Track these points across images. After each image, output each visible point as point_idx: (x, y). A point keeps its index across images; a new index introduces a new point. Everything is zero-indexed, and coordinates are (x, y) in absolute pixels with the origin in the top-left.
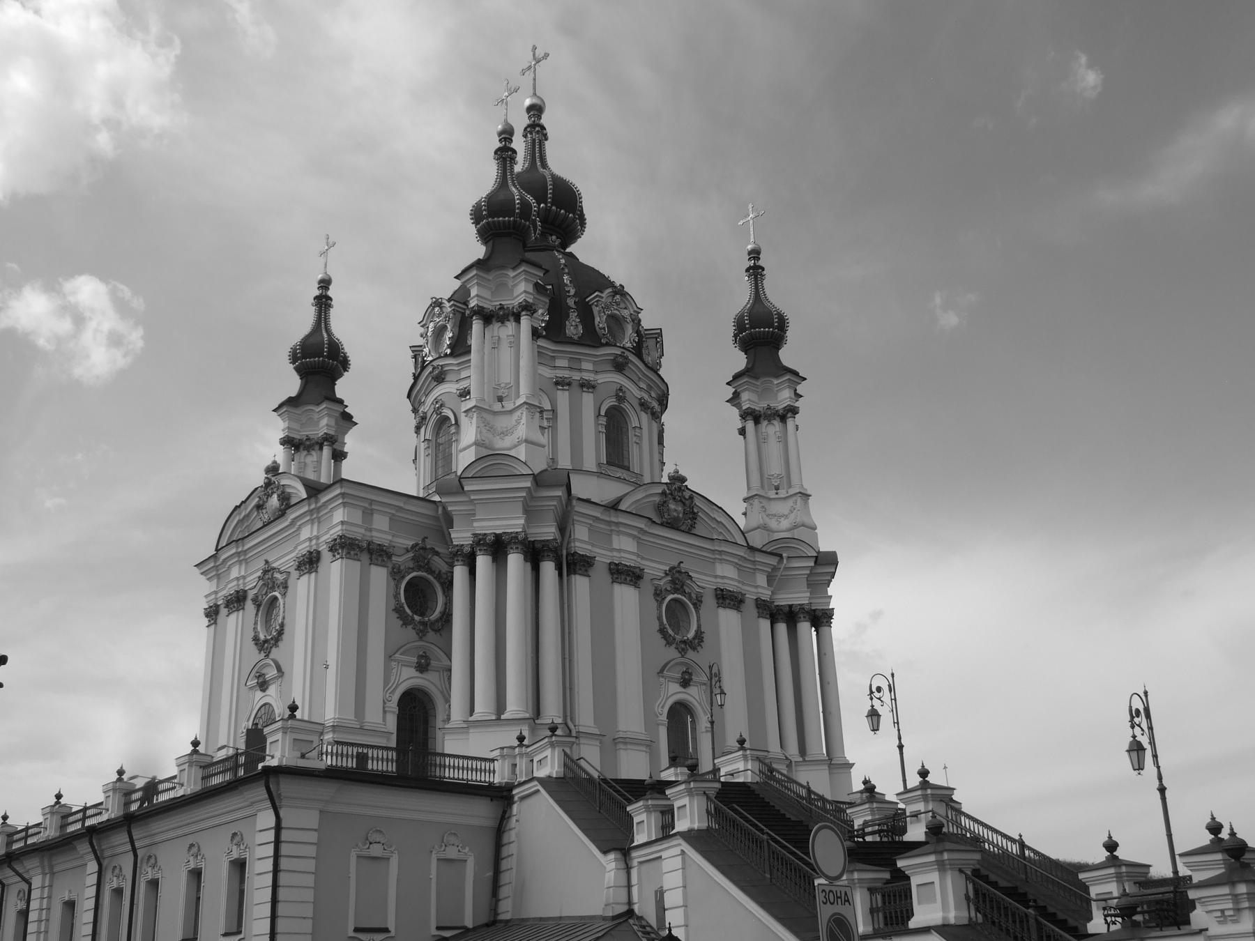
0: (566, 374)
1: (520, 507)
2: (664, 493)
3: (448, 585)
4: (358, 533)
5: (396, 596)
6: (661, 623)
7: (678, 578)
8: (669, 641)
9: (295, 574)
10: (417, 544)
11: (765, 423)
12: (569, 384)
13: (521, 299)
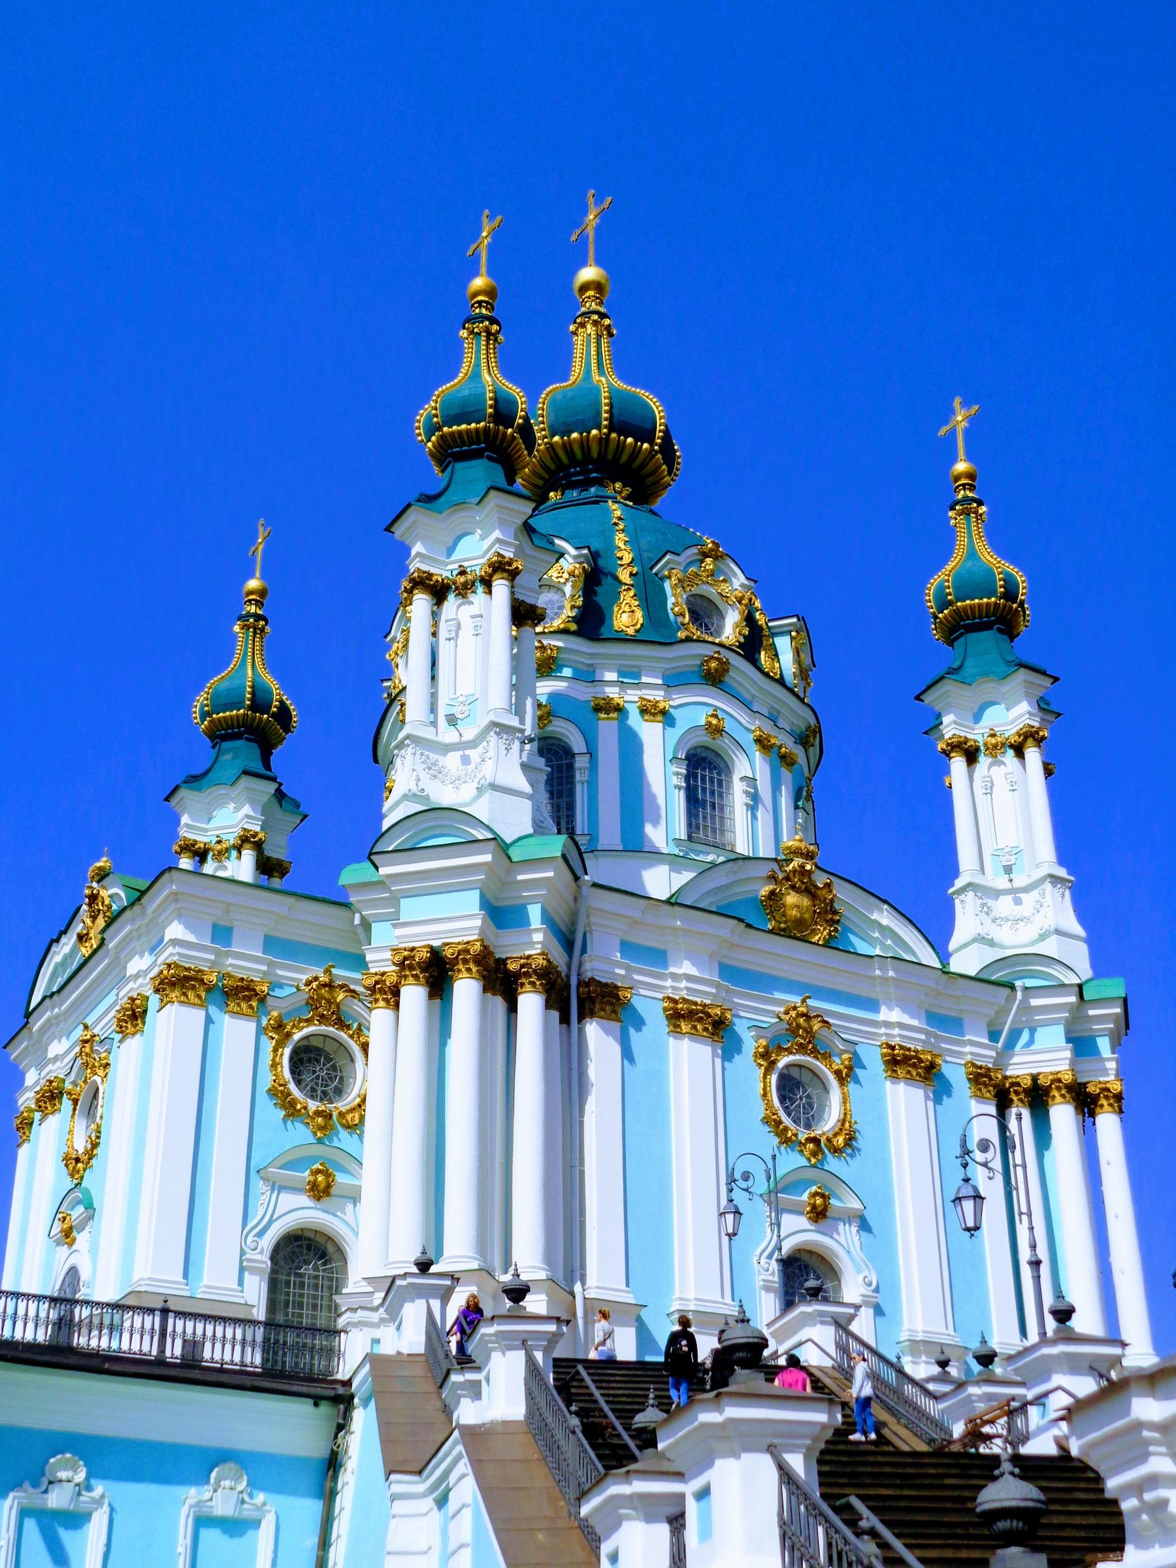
1: (474, 896)
4: (202, 959)
5: (274, 1065)
6: (769, 1106)
10: (316, 979)
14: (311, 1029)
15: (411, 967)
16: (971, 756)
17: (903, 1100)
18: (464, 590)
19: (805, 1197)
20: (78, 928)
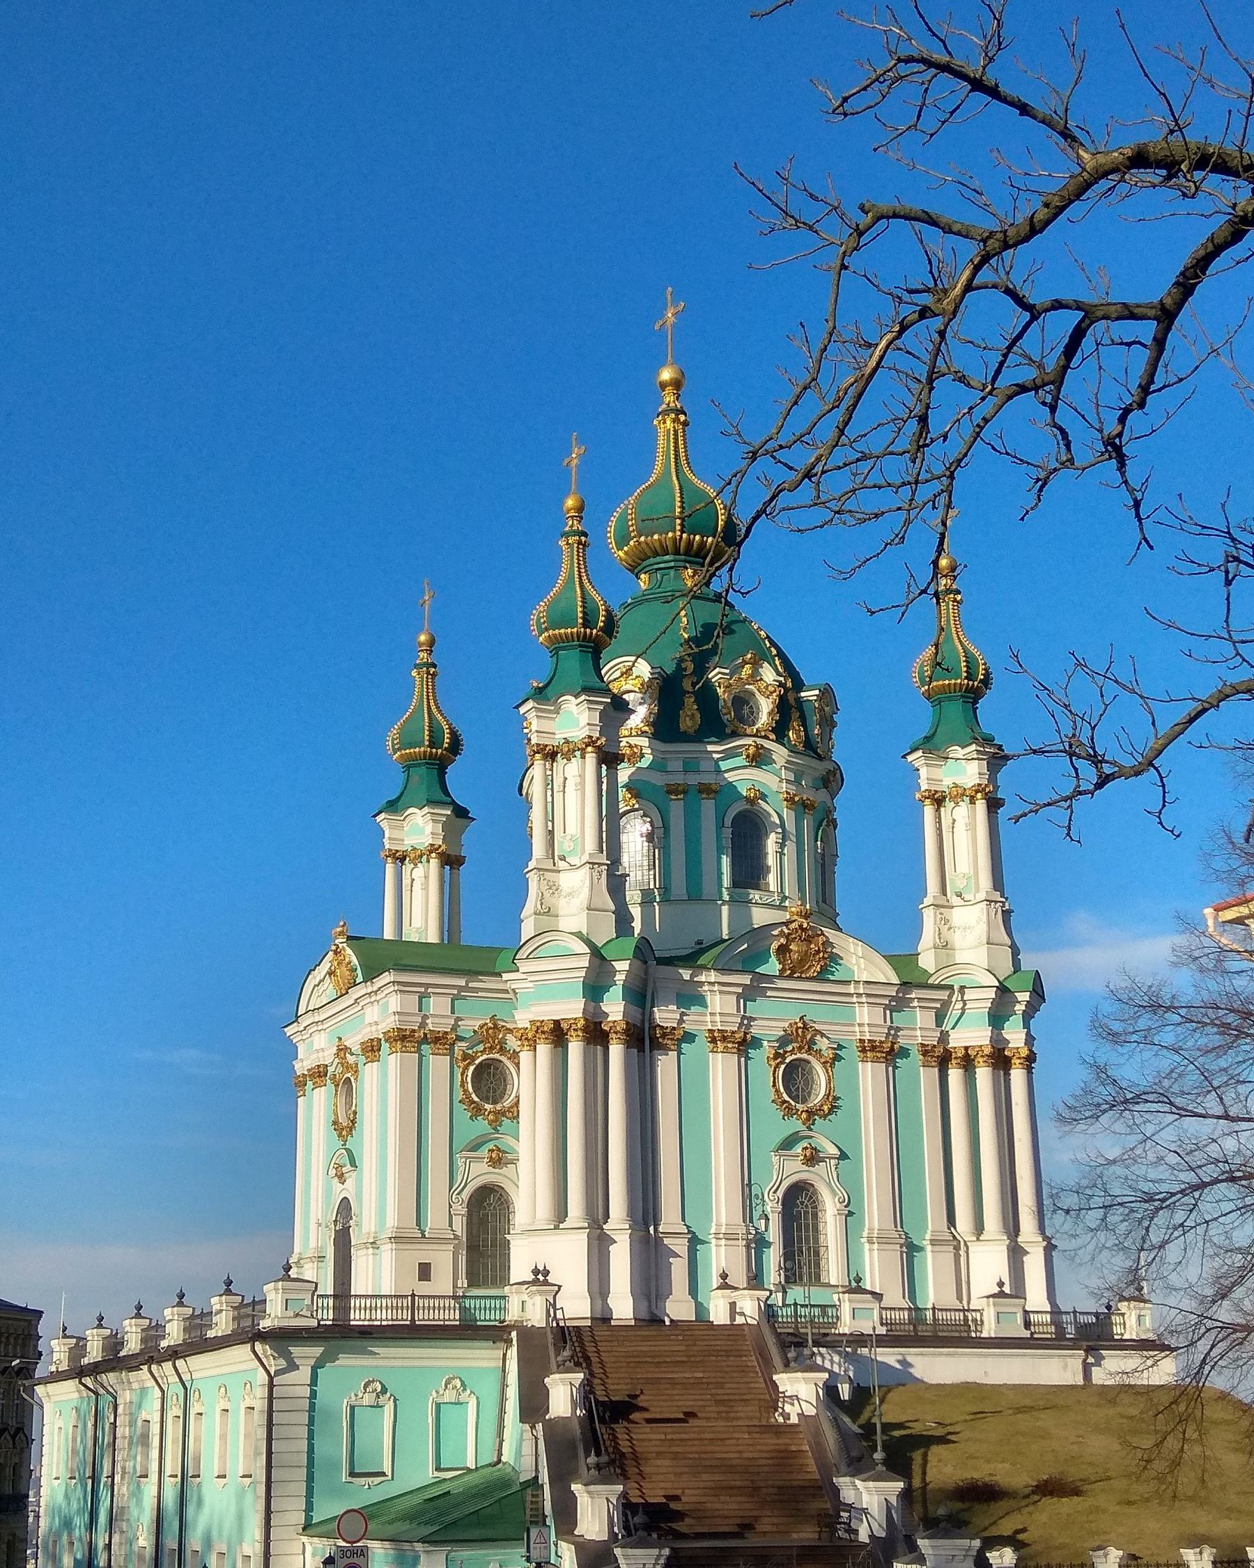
0: (679, 779)
2: (782, 934)
3: (518, 1065)
4: (413, 1023)
5: (462, 1085)
6: (777, 1091)
7: (802, 1035)
8: (789, 1112)
9: (362, 1059)
11: (952, 804)
12: (685, 792)
13: (585, 732)
14: (485, 1057)
15: (543, 1032)
16: (938, 801)
17: (869, 1076)
18: (568, 756)
19: (799, 1151)
20: (325, 967)
